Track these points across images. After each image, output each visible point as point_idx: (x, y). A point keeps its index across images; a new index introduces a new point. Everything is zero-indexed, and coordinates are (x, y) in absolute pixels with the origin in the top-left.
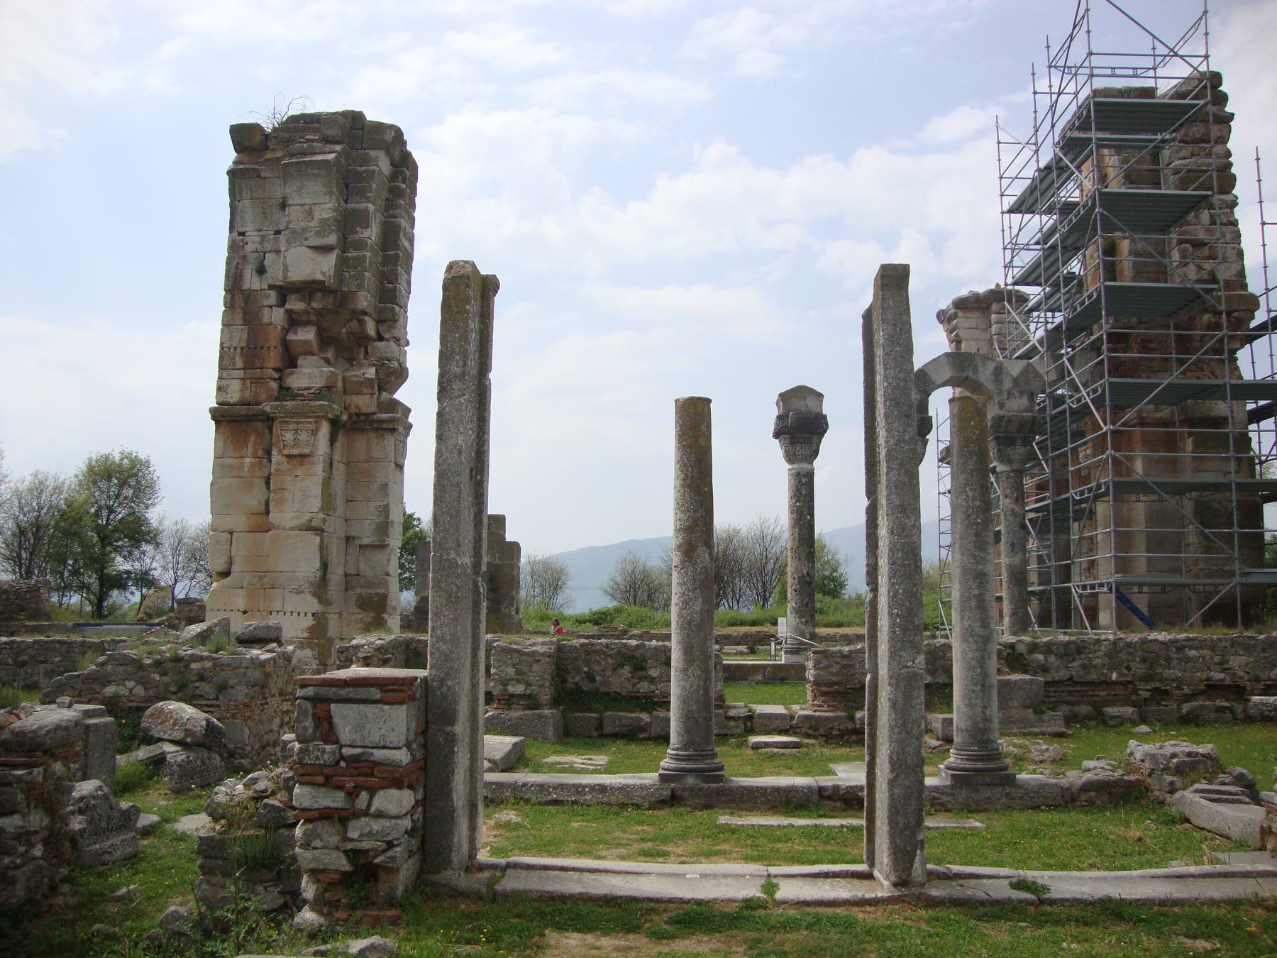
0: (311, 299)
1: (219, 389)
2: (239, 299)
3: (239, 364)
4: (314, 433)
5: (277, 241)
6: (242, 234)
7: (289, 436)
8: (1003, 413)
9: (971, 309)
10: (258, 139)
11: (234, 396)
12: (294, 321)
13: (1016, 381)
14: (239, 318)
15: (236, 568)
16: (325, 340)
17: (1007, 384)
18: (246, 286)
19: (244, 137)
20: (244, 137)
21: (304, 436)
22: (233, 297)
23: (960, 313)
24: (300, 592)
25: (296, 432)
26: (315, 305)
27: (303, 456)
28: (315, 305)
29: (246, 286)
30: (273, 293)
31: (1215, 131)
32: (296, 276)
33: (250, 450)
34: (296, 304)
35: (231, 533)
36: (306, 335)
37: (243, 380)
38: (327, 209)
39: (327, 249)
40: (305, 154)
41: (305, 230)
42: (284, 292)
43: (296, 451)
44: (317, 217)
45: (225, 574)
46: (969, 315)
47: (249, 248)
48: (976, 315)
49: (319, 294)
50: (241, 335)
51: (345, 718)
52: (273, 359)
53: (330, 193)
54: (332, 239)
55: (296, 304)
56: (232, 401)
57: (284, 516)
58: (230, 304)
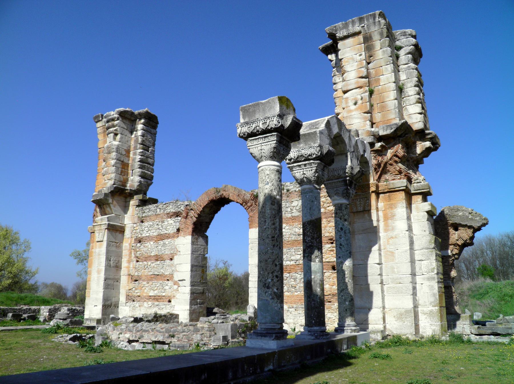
23: (120, 119)
48: (127, 122)
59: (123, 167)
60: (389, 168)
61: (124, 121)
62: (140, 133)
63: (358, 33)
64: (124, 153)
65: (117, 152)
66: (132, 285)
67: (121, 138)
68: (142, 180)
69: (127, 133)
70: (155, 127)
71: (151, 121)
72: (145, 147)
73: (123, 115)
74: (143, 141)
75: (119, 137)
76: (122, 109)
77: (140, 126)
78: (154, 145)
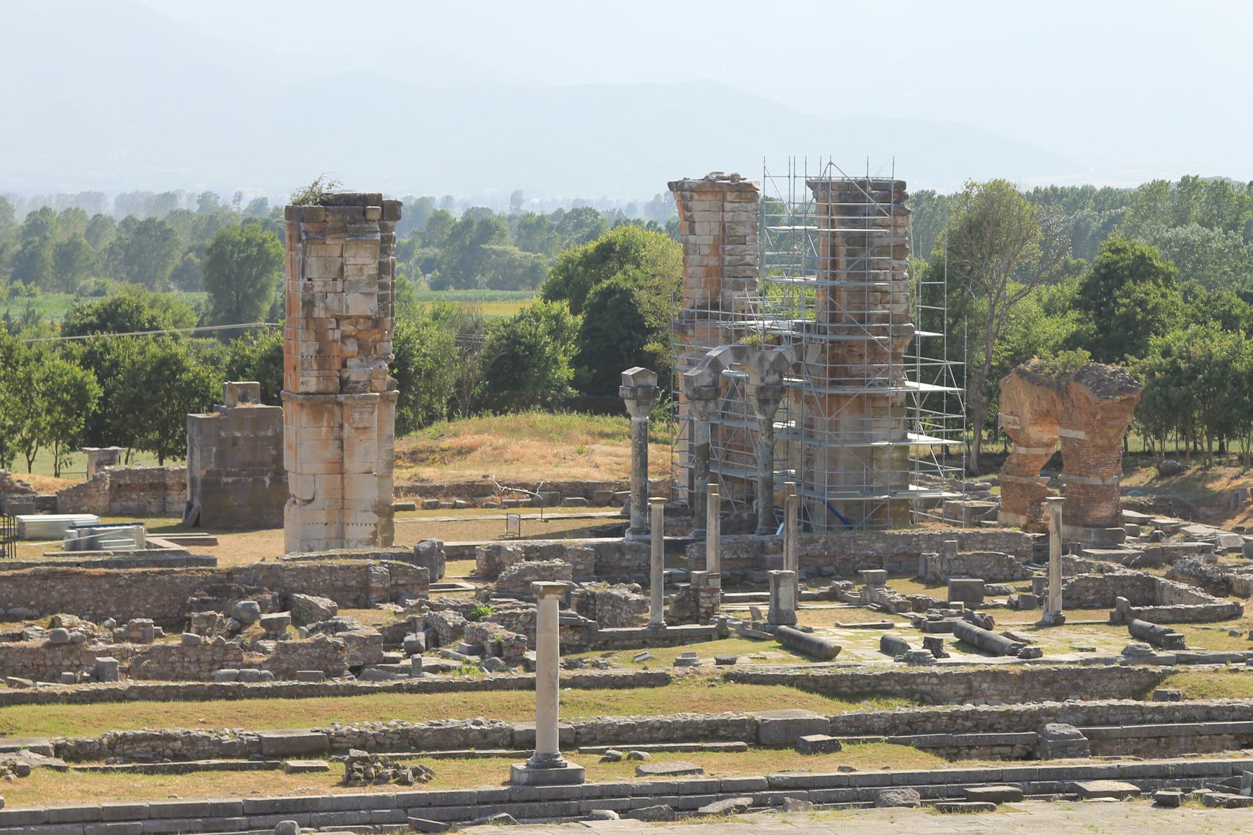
3: (315, 366)
4: (372, 413)
6: (310, 279)
7: (356, 416)
9: (705, 193)
12: (344, 337)
13: (772, 364)
14: (312, 336)
15: (319, 498)
17: (767, 366)
18: (316, 315)
21: (366, 416)
24: (365, 511)
25: (361, 413)
26: (359, 327)
27: (365, 428)
28: (359, 327)
29: (316, 315)
33: (325, 424)
36: (352, 347)
37: (318, 377)
38: (372, 269)
39: (370, 294)
41: (358, 282)
43: (361, 425)
44: (366, 273)
45: (309, 502)
46: (704, 197)
47: (316, 289)
51: (711, 581)
57: (354, 465)
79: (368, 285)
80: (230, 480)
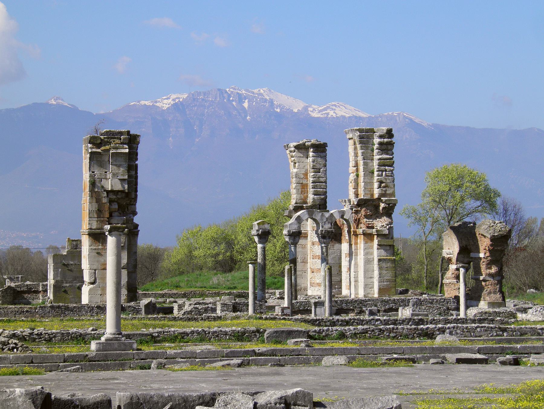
0: (117, 195)
1: (89, 224)
2: (94, 195)
3: (96, 216)
5: (106, 175)
6: (93, 172)
8: (323, 229)
9: (301, 149)
10: (99, 141)
11: (94, 227)
12: (111, 202)
14: (94, 200)
16: (120, 206)
19: (94, 141)
20: (94, 141)
22: (92, 193)
23: (296, 151)
28: (119, 197)
30: (105, 193)
31: (389, 147)
32: (116, 188)
34: (113, 197)
35: (95, 270)
36: (115, 206)
37: (97, 221)
40: (117, 148)
42: (108, 192)
48: (303, 151)
49: (120, 193)
50: (95, 206)
52: (107, 215)
53: (126, 162)
54: (126, 177)
55: (113, 197)
56: (94, 228)
58: (91, 196)
59: (303, 187)
60: (362, 221)
61: (300, 151)
62: (310, 159)
63: (352, 138)
64: (302, 176)
65: (296, 177)
66: (312, 275)
67: (299, 165)
68: (315, 197)
69: (304, 159)
70: (324, 151)
71: (320, 149)
72: (317, 170)
73: (297, 147)
74: (314, 166)
75: (297, 165)
76: (295, 144)
77: (311, 154)
78: (325, 166)
79: (123, 175)
80: (68, 285)
